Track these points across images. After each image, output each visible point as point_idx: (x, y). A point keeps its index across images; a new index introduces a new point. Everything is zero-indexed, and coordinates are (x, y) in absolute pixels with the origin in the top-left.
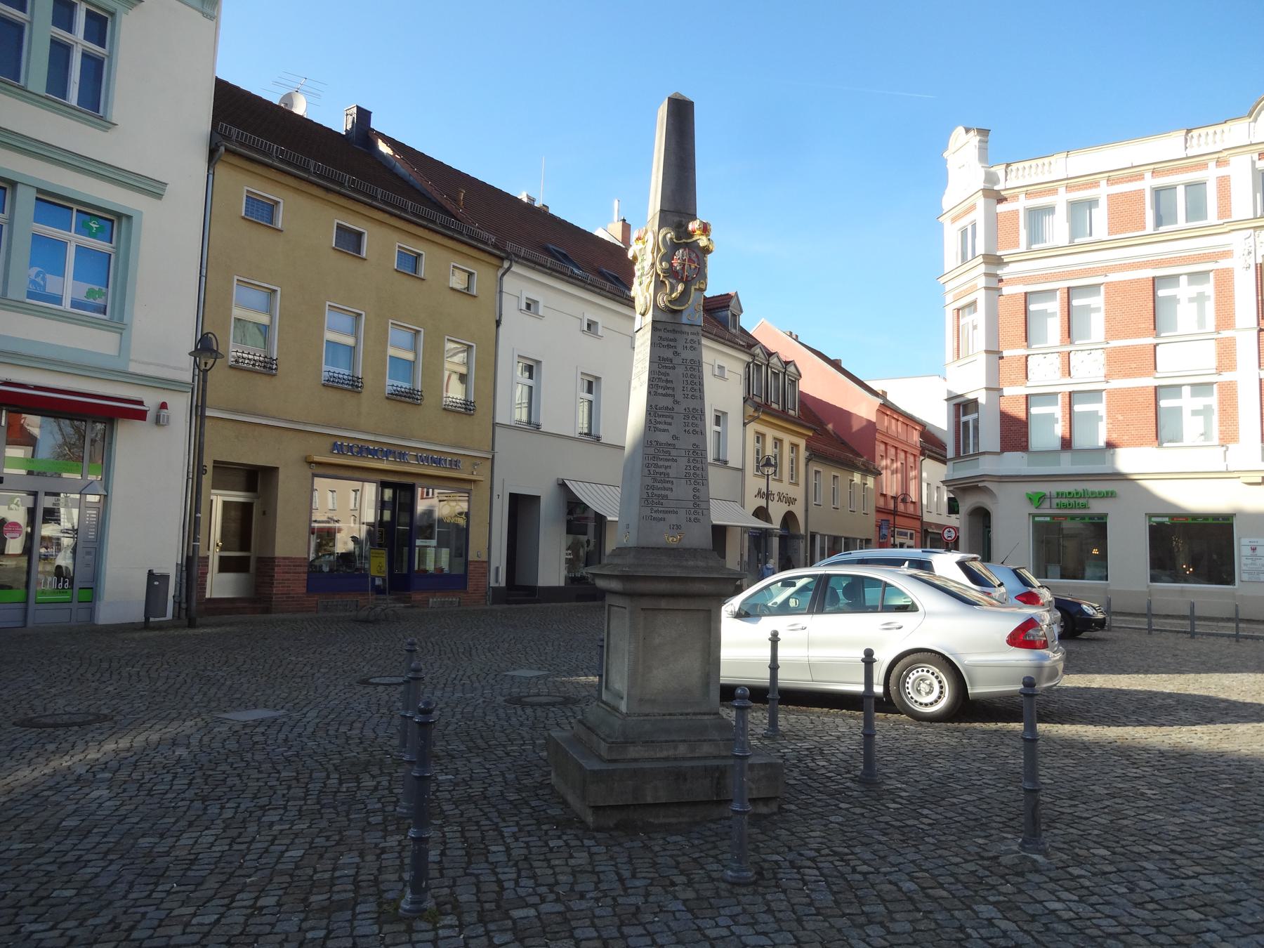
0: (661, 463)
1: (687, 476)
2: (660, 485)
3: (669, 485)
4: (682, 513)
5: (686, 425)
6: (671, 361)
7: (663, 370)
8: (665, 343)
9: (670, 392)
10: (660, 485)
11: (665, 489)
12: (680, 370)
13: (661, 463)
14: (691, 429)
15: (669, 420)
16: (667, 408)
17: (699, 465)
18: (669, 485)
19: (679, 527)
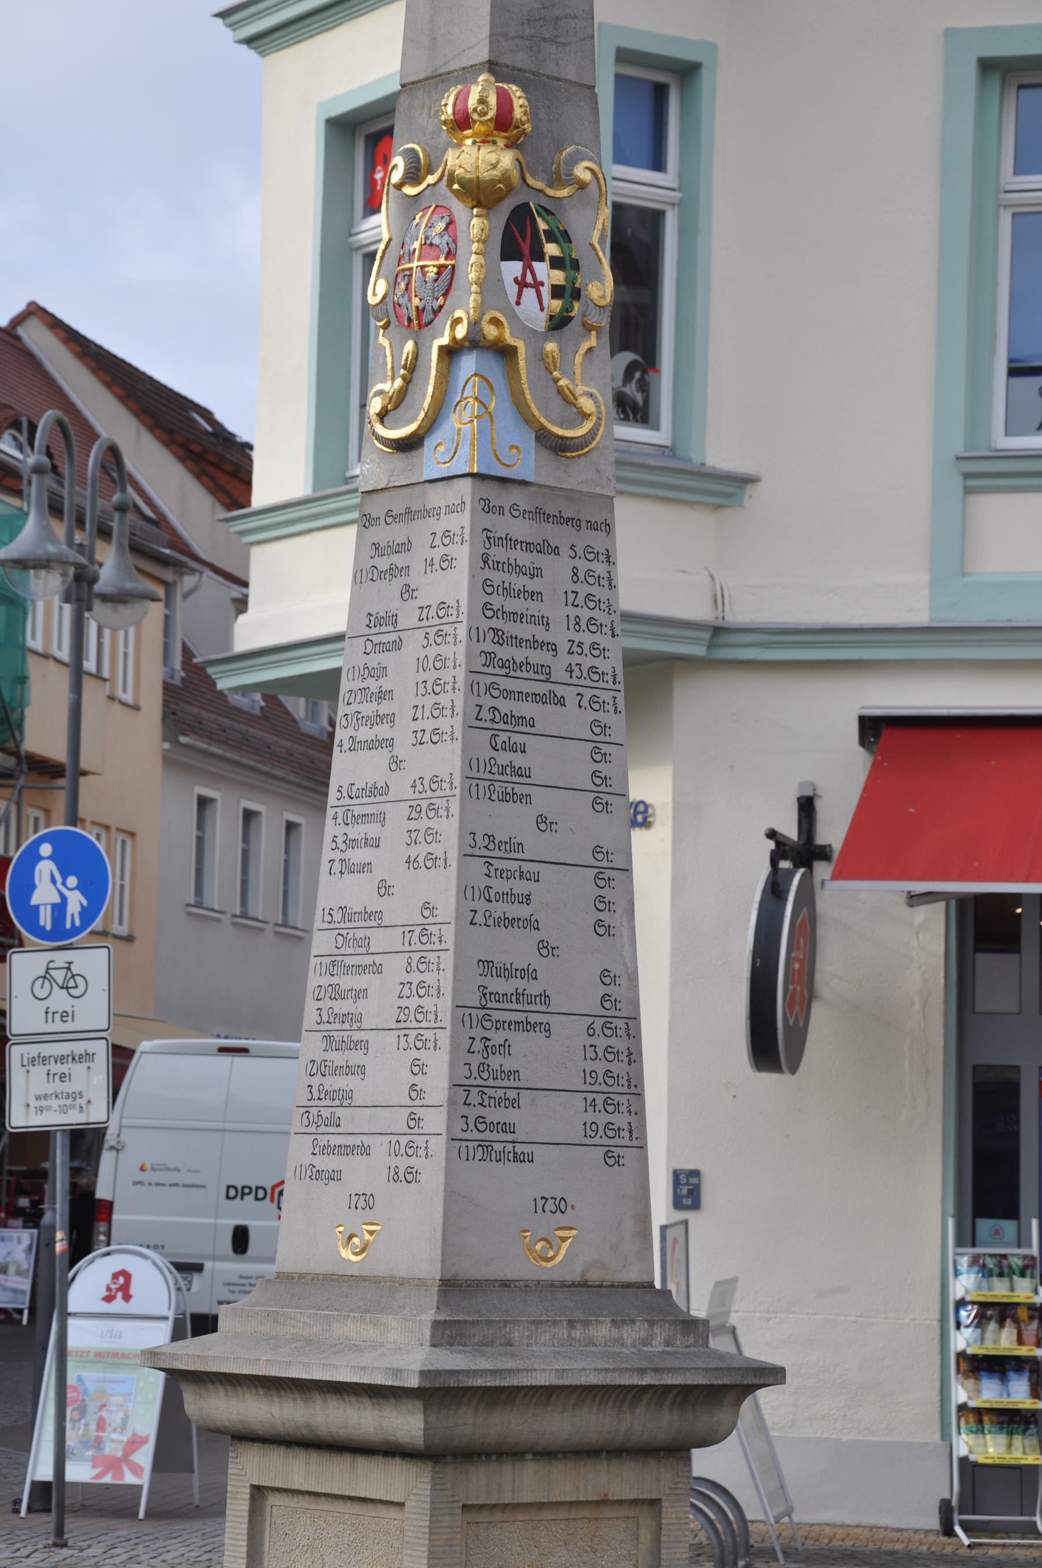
0: (346, 982)
2: (338, 1058)
3: (356, 1057)
4: (379, 1146)
6: (394, 619)
7: (373, 660)
8: (383, 564)
9: (383, 731)
10: (338, 1058)
11: (349, 1070)
12: (413, 647)
13: (346, 982)
15: (372, 830)
16: (375, 791)
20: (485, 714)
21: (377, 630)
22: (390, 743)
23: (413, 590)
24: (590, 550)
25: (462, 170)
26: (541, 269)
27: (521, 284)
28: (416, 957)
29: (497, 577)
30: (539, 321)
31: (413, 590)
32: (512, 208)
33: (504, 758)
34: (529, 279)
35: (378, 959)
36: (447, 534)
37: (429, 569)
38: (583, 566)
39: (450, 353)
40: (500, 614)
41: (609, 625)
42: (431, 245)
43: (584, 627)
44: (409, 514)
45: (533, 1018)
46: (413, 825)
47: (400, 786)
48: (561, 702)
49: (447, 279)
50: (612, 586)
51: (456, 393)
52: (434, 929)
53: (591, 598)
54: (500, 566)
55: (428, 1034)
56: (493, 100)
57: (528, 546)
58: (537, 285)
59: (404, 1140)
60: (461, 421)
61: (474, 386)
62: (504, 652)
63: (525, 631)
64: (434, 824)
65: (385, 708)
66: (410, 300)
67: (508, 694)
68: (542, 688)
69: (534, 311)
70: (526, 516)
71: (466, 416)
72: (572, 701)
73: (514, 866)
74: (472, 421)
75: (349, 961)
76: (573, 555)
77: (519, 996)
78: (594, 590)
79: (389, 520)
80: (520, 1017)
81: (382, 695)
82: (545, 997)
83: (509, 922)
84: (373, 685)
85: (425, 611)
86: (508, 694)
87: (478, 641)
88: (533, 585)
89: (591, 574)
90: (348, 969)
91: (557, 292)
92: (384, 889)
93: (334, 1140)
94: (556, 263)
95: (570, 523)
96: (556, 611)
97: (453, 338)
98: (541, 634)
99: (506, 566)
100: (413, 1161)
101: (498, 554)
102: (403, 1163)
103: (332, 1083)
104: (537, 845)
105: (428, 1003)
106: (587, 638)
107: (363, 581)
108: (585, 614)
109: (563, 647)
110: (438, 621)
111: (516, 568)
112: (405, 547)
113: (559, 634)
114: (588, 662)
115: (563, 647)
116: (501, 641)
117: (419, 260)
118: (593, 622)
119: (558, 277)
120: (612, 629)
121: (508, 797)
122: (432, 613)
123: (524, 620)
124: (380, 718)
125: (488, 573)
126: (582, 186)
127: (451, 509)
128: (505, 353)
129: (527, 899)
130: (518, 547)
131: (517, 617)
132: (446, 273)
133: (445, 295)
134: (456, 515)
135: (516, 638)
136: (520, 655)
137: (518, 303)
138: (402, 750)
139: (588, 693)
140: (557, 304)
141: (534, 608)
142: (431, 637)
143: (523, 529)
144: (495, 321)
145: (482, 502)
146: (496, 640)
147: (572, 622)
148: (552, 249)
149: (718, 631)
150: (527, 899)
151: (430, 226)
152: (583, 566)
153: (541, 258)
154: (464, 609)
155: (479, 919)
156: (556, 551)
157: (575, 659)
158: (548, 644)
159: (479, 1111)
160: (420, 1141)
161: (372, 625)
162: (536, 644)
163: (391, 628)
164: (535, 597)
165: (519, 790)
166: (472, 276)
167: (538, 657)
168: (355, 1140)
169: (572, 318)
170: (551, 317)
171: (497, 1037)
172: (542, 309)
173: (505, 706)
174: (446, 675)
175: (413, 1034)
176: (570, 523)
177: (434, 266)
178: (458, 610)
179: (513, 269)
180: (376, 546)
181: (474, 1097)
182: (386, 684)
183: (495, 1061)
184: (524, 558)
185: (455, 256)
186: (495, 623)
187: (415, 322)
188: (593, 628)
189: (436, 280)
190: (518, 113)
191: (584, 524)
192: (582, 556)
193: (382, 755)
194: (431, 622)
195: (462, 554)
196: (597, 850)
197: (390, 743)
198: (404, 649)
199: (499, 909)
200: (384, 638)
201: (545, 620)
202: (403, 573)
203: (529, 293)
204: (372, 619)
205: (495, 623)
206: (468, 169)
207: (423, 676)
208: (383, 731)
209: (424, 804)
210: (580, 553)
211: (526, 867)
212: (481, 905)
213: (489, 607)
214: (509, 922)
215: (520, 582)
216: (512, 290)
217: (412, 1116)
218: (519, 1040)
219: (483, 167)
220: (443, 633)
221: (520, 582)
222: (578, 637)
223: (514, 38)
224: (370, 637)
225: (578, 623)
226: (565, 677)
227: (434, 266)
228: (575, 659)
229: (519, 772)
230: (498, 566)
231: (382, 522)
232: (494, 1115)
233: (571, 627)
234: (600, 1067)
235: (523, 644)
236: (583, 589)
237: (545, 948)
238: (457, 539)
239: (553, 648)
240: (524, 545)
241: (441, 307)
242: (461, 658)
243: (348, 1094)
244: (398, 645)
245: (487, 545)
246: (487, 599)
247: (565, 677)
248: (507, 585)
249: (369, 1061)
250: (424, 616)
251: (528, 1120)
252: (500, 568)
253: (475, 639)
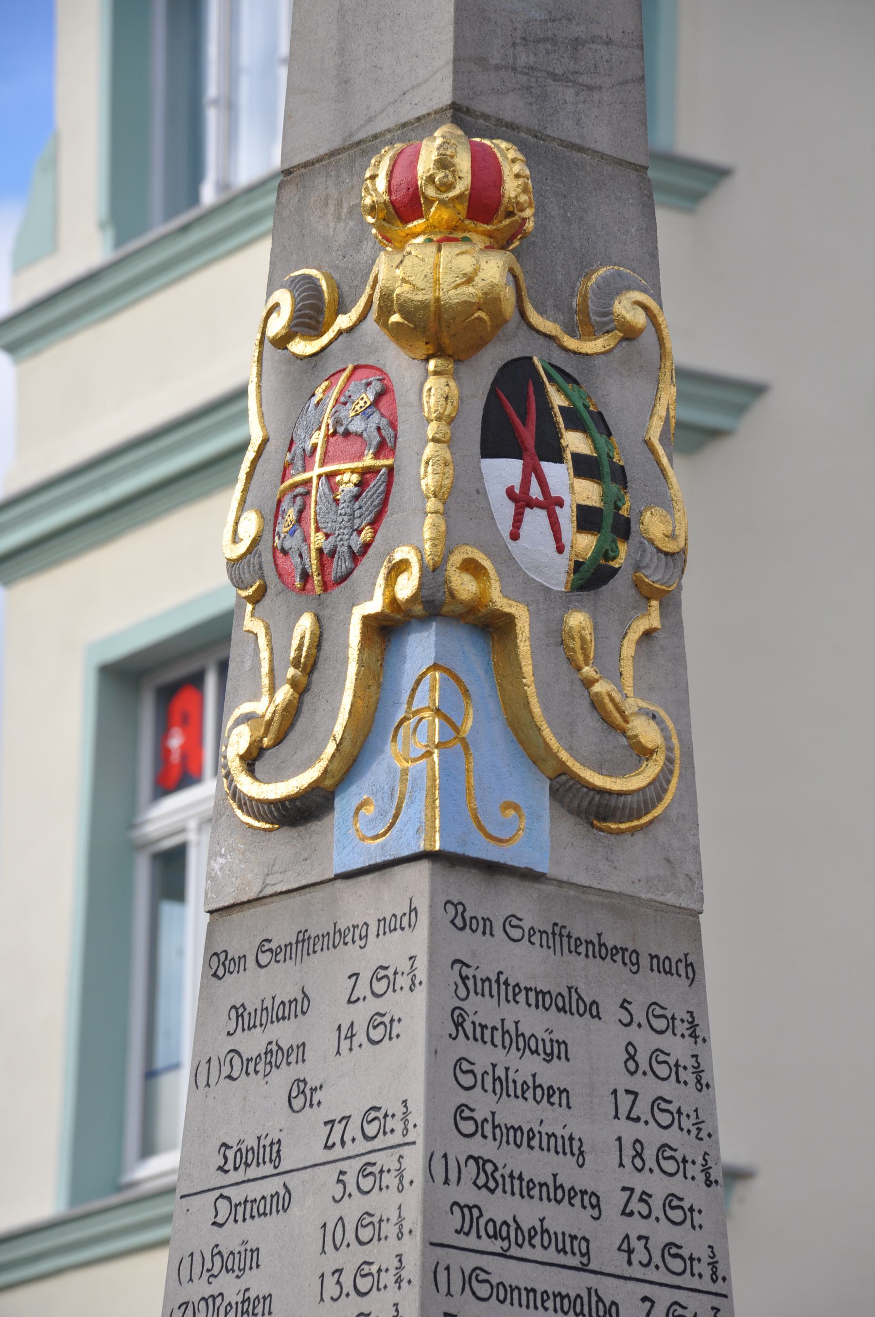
7: (231, 1238)
8: (252, 1044)
21: (239, 1176)
23: (313, 1090)
24: (658, 1011)
25: (406, 287)
27: (521, 501)
29: (483, 1056)
31: (313, 1090)
32: (501, 363)
34: (535, 491)
36: (382, 973)
37: (345, 1045)
38: (646, 1042)
39: (385, 630)
40: (488, 1128)
41: (700, 1160)
42: (347, 434)
43: (651, 1163)
44: (306, 943)
49: (378, 493)
50: (702, 1085)
51: (396, 704)
53: (663, 1106)
54: (487, 1033)
56: (464, 163)
57: (541, 998)
58: (551, 504)
60: (409, 755)
61: (432, 689)
62: (499, 1207)
63: (536, 1165)
66: (306, 539)
69: (546, 553)
70: (536, 939)
71: (418, 746)
74: (429, 754)
76: (627, 1020)
78: (667, 1089)
79: (264, 959)
85: (338, 1128)
87: (446, 1181)
88: (551, 1074)
89: (662, 1057)
95: (618, 958)
96: (598, 1130)
97: (393, 601)
98: (570, 1175)
99: (498, 1035)
101: (484, 1010)
106: (658, 1186)
107: (212, 1081)
108: (652, 1137)
109: (613, 1201)
110: (363, 1146)
112: (297, 1006)
113: (605, 1176)
114: (662, 1233)
115: (613, 1201)
116: (492, 1184)
117: (323, 464)
118: (668, 1153)
119: (588, 492)
120: (706, 1170)
122: (353, 1129)
123: (535, 1143)
125: (463, 1047)
126: (630, 334)
127: (389, 925)
130: (521, 997)
131: (521, 1136)
133: (375, 523)
134: (400, 936)
135: (521, 1178)
136: (529, 1212)
137: (515, 536)
141: (553, 1120)
142: (350, 1179)
143: (528, 964)
144: (471, 567)
145: (450, 907)
146: (481, 1181)
147: (629, 1152)
148: (575, 442)
152: (646, 1042)
154: (418, 1116)
156: (593, 1010)
157: (636, 1227)
158: (584, 1192)
161: (230, 1166)
163: (268, 1169)
164: (555, 1099)
166: (428, 482)
167: (564, 1219)
169: (615, 571)
170: (578, 565)
172: (560, 549)
174: (382, 1255)
176: (618, 958)
177: (353, 471)
178: (405, 1120)
179: (505, 472)
180: (238, 1011)
184: (534, 1022)
185: (393, 450)
187: (316, 579)
188: (670, 1166)
189: (356, 497)
190: (511, 188)
191: (645, 961)
192: (644, 1022)
194: (351, 1149)
195: (413, 1010)
198: (294, 1209)
200: (254, 1191)
201: (576, 1144)
202: (293, 1058)
203: (536, 519)
204: (230, 1154)
206: (420, 284)
207: (334, 1260)
210: (640, 1016)
213: (467, 1113)
215: (526, 1067)
219: (446, 280)
220: (376, 1169)
221: (526, 1067)
222: (640, 1183)
223: (497, 68)
224: (225, 1192)
225: (639, 1155)
227: (353, 471)
228: (636, 1227)
230: (482, 1033)
231: (251, 963)
233: (627, 1161)
235: (535, 1192)
238: (403, 981)
240: (532, 995)
241: (367, 546)
242: (413, 1217)
245: (462, 992)
246: (464, 1097)
248: (500, 1072)
250: (336, 1138)
252: (487, 1038)
253: (440, 1177)
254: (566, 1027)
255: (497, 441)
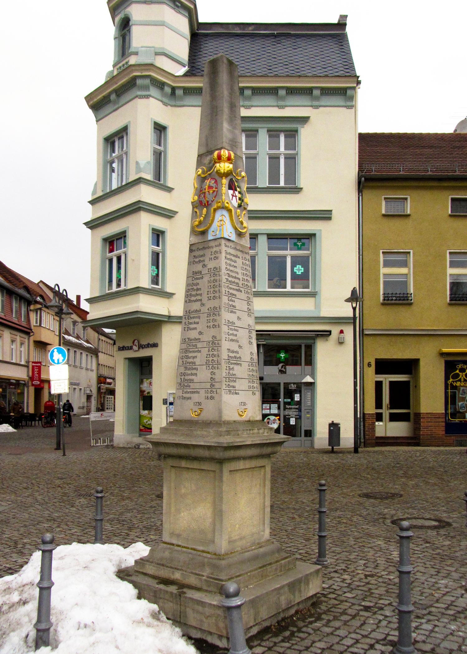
0: (190, 355)
1: (207, 363)
2: (189, 372)
3: (194, 372)
4: (202, 392)
5: (208, 321)
6: (201, 272)
7: (195, 282)
9: (199, 298)
10: (189, 372)
11: (192, 374)
12: (206, 278)
13: (190, 355)
14: (211, 324)
15: (197, 320)
16: (196, 311)
17: (215, 353)
18: (194, 372)
19: (200, 404)
20: (227, 293)
22: (201, 300)
26: (237, 193)
27: (233, 196)
28: (211, 348)
30: (236, 205)
33: (231, 303)
35: (199, 349)
38: (244, 262)
44: (204, 248)
45: (238, 362)
46: (208, 318)
47: (204, 309)
48: (241, 291)
52: (216, 342)
55: (216, 366)
57: (234, 256)
58: (236, 196)
59: (209, 390)
62: (230, 279)
63: (234, 275)
64: (215, 318)
65: (199, 292)
67: (231, 288)
68: (237, 288)
72: (243, 291)
73: (233, 328)
75: (191, 350)
77: (235, 357)
80: (235, 362)
81: (198, 290)
82: (240, 357)
83: (232, 340)
84: (195, 288)
86: (231, 288)
88: (235, 264)
90: (191, 352)
91: (240, 199)
92: (201, 333)
93: (188, 390)
94: (240, 193)
98: (237, 276)
100: (212, 395)
101: (228, 256)
102: (209, 395)
103: (186, 377)
104: (238, 323)
105: (215, 359)
106: (246, 278)
108: (245, 272)
111: (231, 260)
113: (240, 276)
114: (246, 283)
121: (232, 312)
122: (212, 269)
124: (197, 295)
128: (230, 211)
129: (236, 335)
132: (215, 192)
133: (215, 197)
136: (233, 280)
138: (205, 300)
139: (246, 290)
140: (240, 202)
141: (235, 270)
143: (233, 252)
144: (227, 203)
148: (238, 189)
149: (169, 317)
150: (236, 335)
151: (210, 182)
152: (244, 262)
153: (236, 190)
155: (227, 339)
156: (239, 257)
157: (243, 282)
159: (229, 383)
160: (215, 390)
162: (235, 278)
165: (234, 310)
167: (236, 281)
168: (196, 390)
171: (232, 366)
173: (231, 291)
175: (211, 366)
179: (231, 192)
181: (227, 380)
182: (198, 287)
183: (231, 372)
184: (233, 258)
186: (228, 272)
193: (199, 303)
196: (249, 325)
197: (201, 300)
199: (231, 337)
200: (198, 277)
203: (234, 198)
205: (228, 272)
208: (199, 298)
209: (212, 313)
211: (236, 328)
212: (227, 336)
214: (232, 340)
215: (233, 263)
216: (231, 197)
217: (211, 384)
218: (236, 367)
221: (233, 263)
222: (244, 277)
226: (241, 286)
228: (243, 282)
229: (234, 306)
230: (228, 259)
232: (231, 384)
234: (251, 373)
236: (245, 267)
237: (240, 347)
239: (239, 279)
243: (193, 380)
244: (202, 278)
247: (241, 286)
249: (198, 372)
251: (238, 385)
254: (237, 259)
255: (230, 188)
